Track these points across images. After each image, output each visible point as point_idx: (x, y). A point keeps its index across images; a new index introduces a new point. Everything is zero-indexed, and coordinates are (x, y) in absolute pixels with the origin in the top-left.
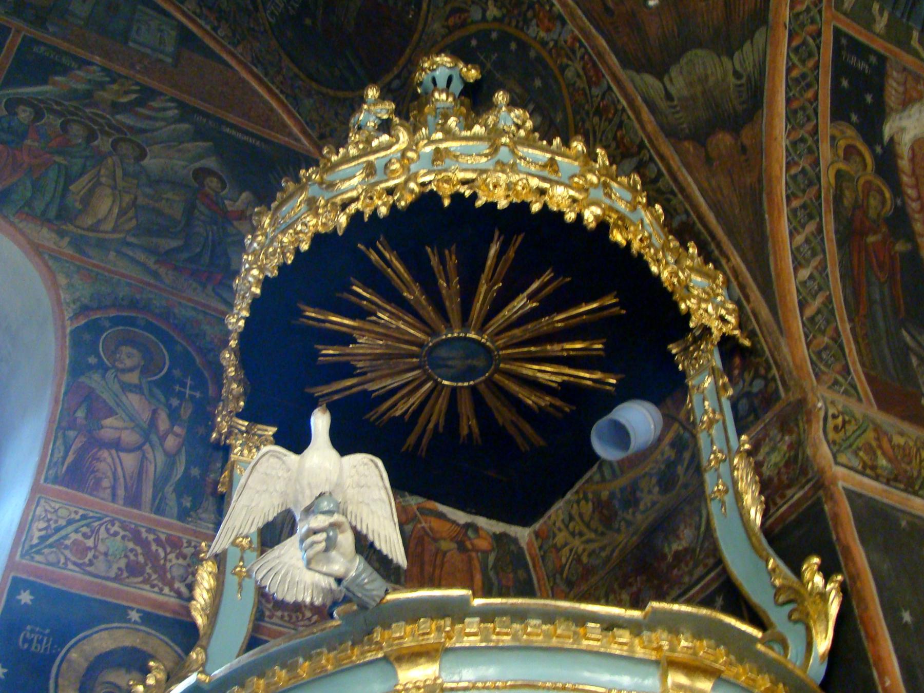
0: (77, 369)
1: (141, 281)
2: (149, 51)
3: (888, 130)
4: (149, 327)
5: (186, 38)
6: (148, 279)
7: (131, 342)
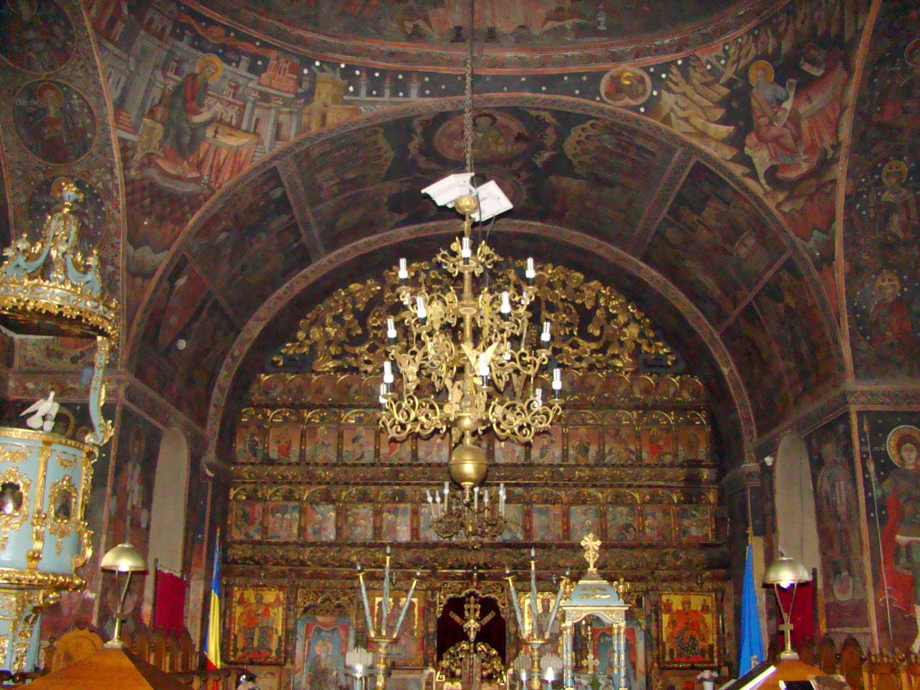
3: (176, 283)
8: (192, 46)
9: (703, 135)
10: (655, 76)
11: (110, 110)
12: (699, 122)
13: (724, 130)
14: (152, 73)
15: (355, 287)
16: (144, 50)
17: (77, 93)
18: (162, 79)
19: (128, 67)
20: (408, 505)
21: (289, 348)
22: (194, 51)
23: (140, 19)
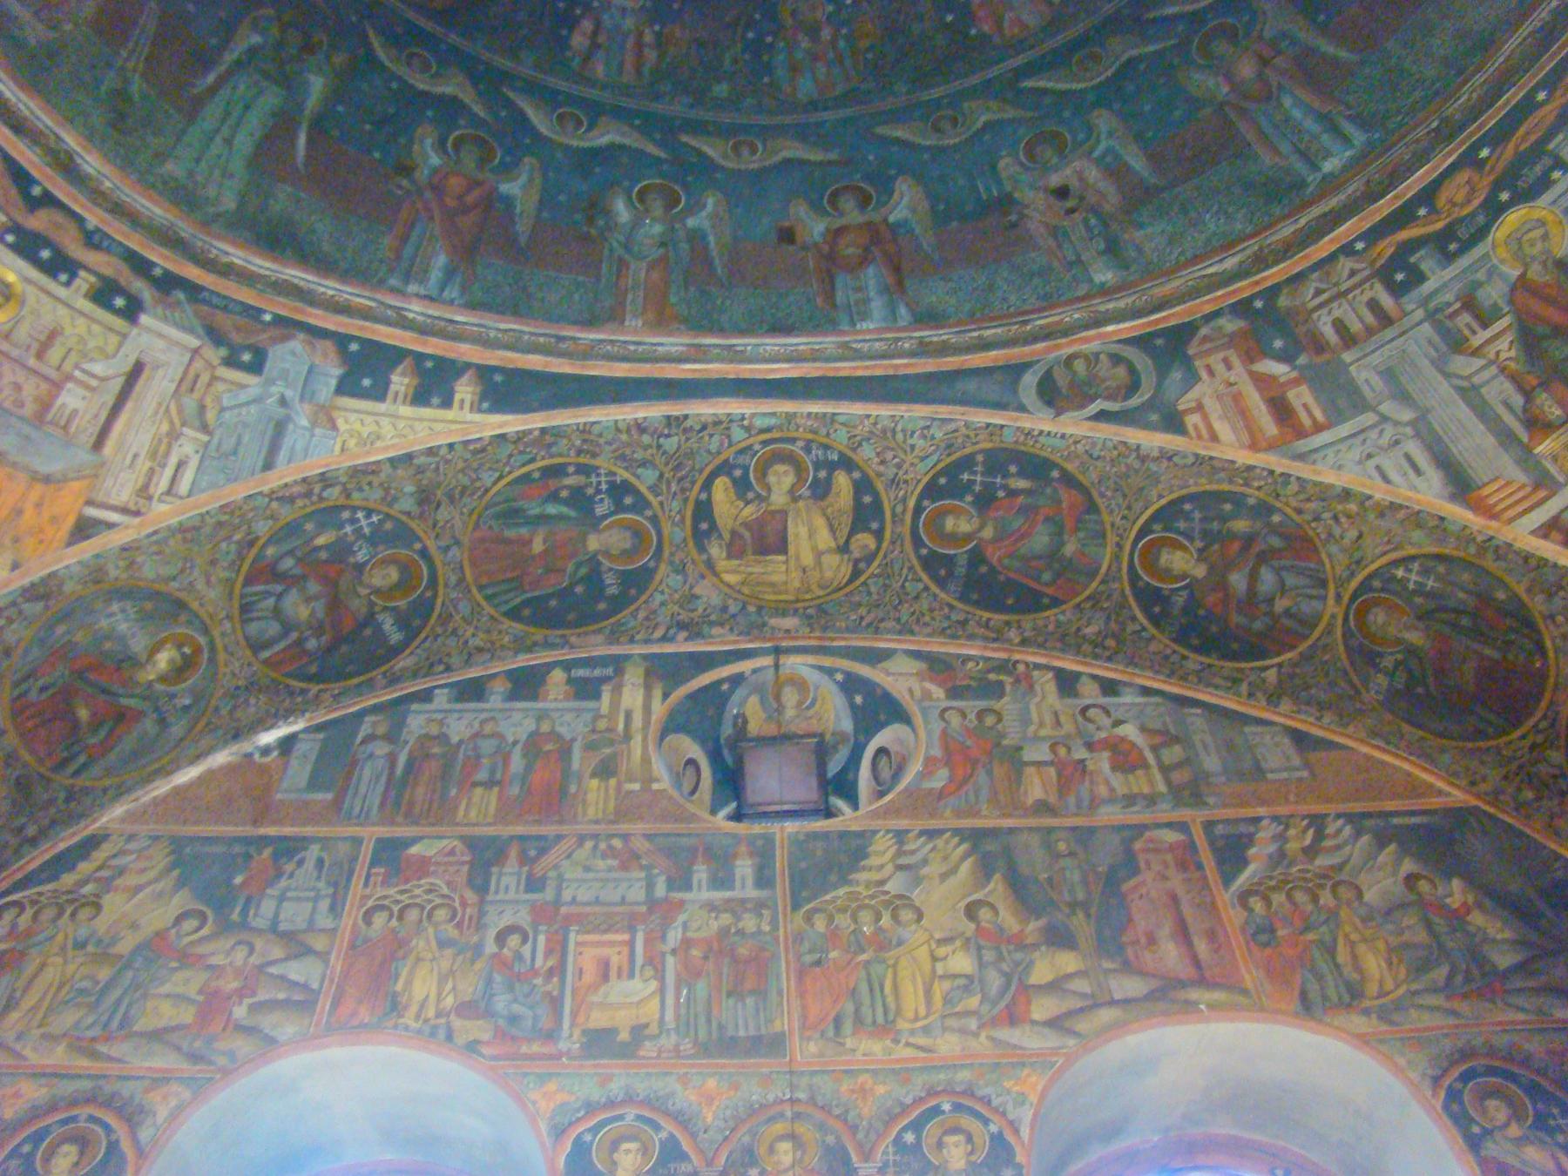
0: (1474, 1144)
1: (1457, 1026)
2: (1285, 775)
4: (1491, 1071)
5: (1300, 739)
6: (1451, 1021)
7: (1495, 1093)
8: (1449, 258)
11: (1459, 514)
14: (1446, 375)
16: (1388, 374)
17: (1395, 563)
18: (1478, 363)
19: (1397, 423)
22: (1464, 261)
23: (1319, 346)
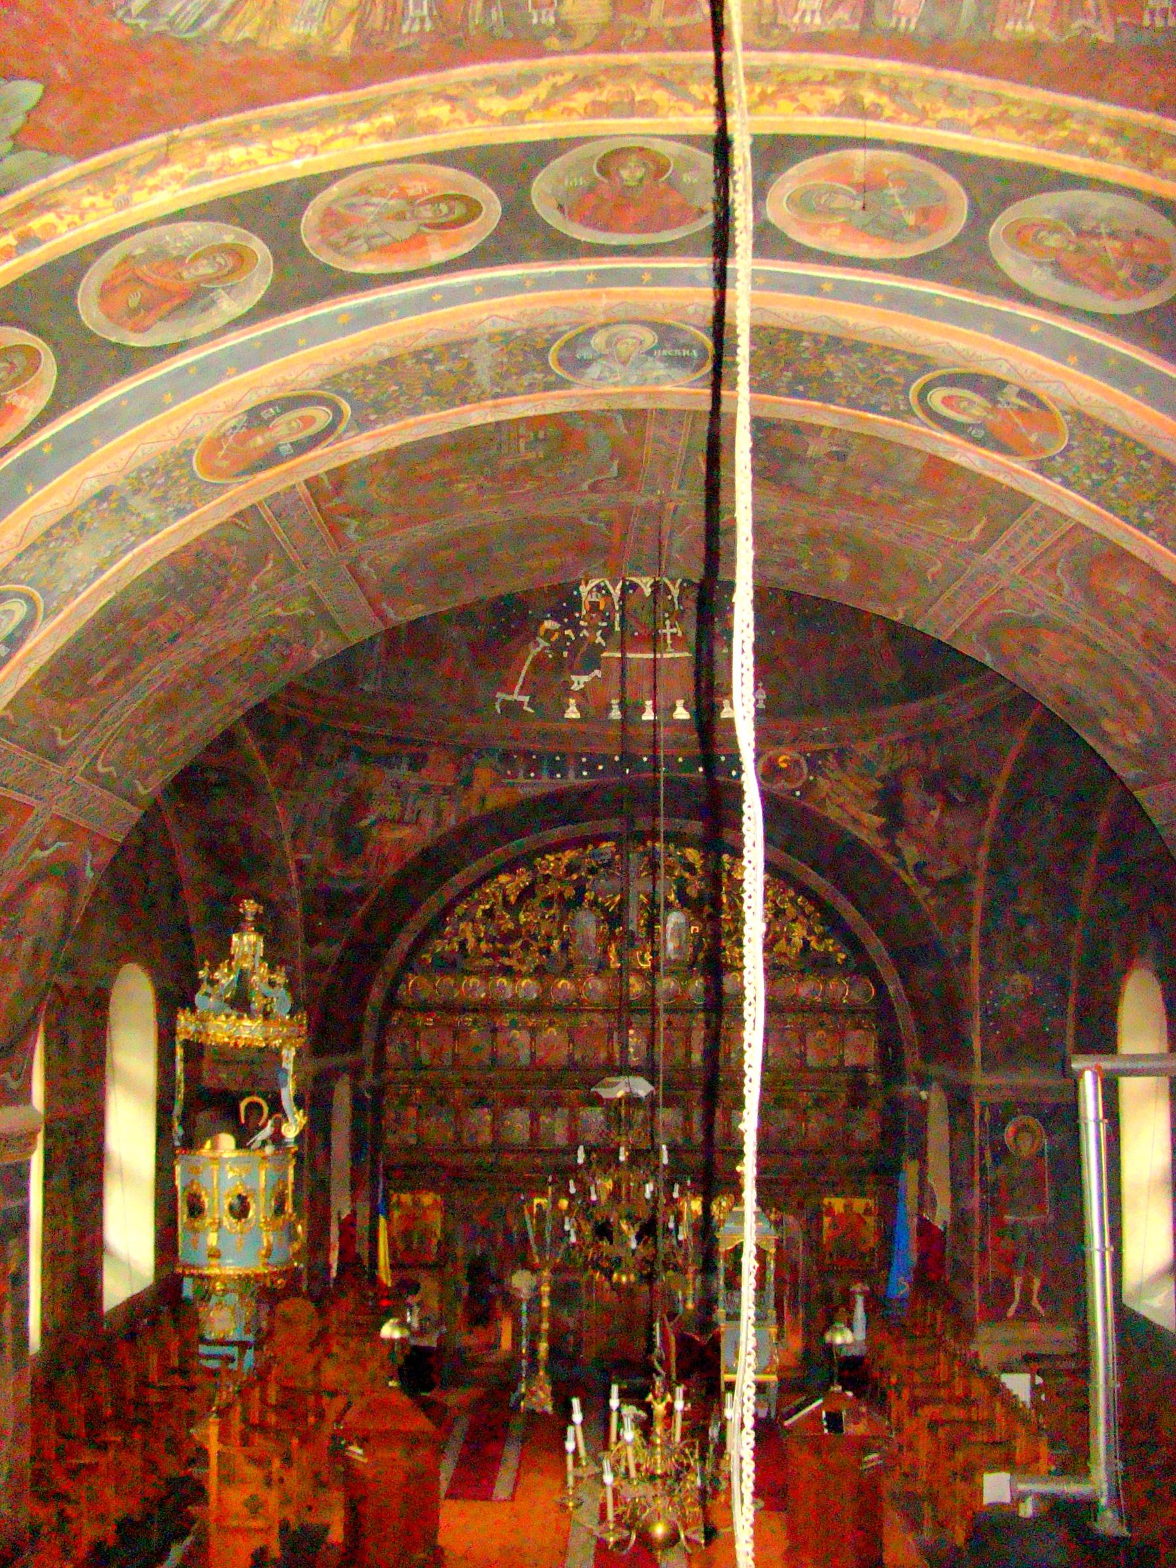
9: (855, 821)
10: (811, 763)
12: (853, 809)
13: (877, 821)
15: (503, 879)
20: (566, 1111)
21: (440, 946)
